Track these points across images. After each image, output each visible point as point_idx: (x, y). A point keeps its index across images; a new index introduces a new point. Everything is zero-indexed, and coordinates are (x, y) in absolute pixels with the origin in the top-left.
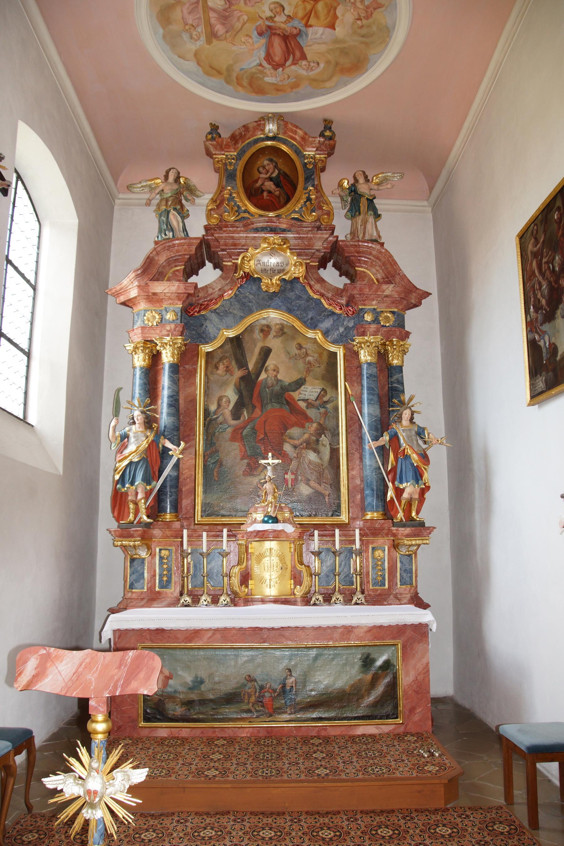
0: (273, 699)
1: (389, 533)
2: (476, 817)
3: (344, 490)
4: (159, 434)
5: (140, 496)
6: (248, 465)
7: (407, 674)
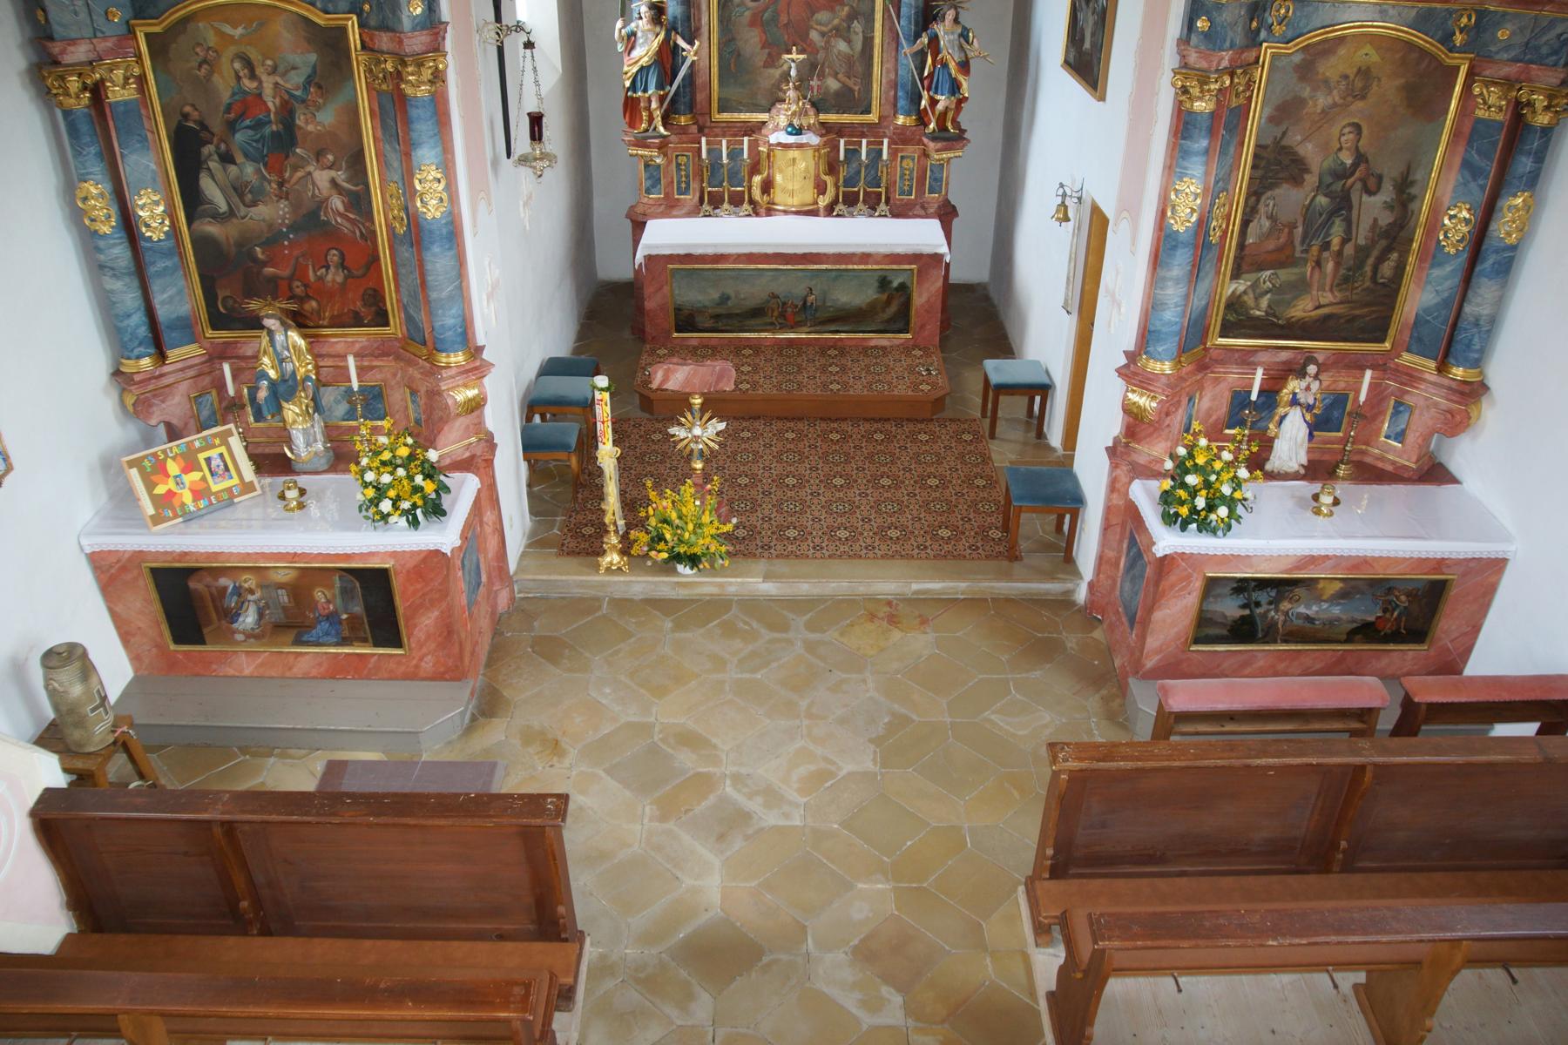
0: (794, 314)
1: (920, 142)
2: (952, 427)
3: (875, 87)
4: (672, 29)
5: (654, 105)
6: (769, 54)
7: (920, 295)
